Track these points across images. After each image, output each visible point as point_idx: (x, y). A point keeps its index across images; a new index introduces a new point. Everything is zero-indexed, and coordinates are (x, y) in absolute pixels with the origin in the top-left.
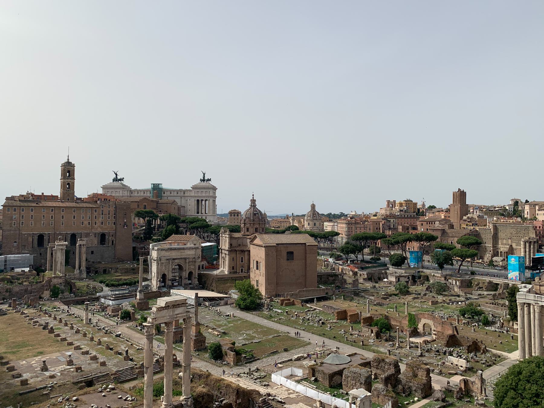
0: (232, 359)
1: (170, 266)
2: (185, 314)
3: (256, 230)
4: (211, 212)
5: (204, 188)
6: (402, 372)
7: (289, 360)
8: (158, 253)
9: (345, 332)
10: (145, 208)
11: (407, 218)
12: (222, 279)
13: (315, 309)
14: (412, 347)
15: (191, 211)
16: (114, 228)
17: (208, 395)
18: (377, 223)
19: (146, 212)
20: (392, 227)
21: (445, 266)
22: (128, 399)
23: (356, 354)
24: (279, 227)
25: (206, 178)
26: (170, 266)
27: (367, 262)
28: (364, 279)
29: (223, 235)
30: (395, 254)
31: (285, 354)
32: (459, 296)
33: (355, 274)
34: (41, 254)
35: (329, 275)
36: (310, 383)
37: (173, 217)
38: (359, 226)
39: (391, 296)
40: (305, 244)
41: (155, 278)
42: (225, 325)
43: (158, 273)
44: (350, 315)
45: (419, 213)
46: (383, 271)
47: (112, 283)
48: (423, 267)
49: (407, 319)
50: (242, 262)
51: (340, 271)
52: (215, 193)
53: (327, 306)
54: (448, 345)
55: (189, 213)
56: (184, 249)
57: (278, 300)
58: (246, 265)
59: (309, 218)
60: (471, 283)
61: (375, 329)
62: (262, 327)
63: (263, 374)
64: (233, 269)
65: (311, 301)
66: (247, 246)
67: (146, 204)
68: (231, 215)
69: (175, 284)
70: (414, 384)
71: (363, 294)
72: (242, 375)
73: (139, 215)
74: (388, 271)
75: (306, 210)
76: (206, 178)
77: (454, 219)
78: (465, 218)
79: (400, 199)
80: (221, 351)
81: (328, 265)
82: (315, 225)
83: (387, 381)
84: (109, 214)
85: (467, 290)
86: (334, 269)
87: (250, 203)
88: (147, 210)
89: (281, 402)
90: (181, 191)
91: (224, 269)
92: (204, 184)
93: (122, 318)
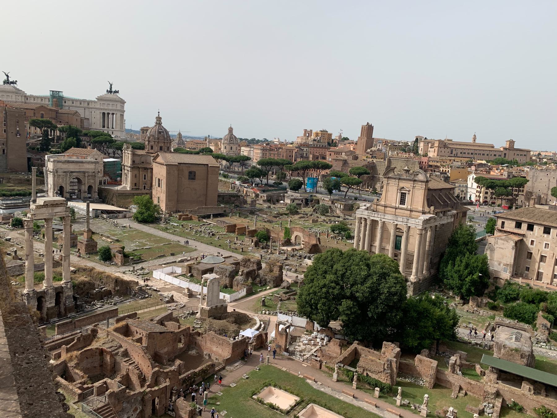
1: (68, 179)
3: (161, 149)
4: (118, 127)
5: (111, 101)
7: (173, 262)
8: (54, 165)
9: (230, 242)
10: (42, 117)
11: (319, 147)
12: (124, 195)
13: (210, 224)
14: (282, 253)
15: (96, 124)
16: (5, 136)
17: (89, 283)
18: (291, 151)
19: (43, 122)
20: (305, 155)
21: (334, 191)
23: (231, 256)
24: (195, 149)
25: (113, 90)
26: (68, 179)
27: (271, 186)
28: (264, 201)
29: (126, 152)
30: (294, 180)
31: (172, 257)
32: (339, 217)
33: (257, 196)
35: (232, 196)
36: (187, 278)
37: (73, 129)
38: (272, 152)
39: (282, 215)
41: (52, 190)
42: (120, 234)
43: (54, 185)
45: (332, 143)
46: (282, 195)
47: (4, 192)
48: (317, 192)
49: (284, 232)
50: (145, 179)
51: (245, 193)
52: (123, 107)
53: (221, 221)
54: (310, 252)
55: (94, 127)
56: (82, 162)
57: (177, 215)
58: (149, 183)
59: (226, 142)
60: (353, 207)
61: (255, 239)
62: (155, 236)
63: (146, 271)
65: (208, 217)
66: (150, 164)
67: (43, 112)
68: (143, 133)
69: (73, 197)
70: (269, 277)
71: (258, 213)
72: (127, 272)
73: (34, 123)
74: (286, 194)
75: (223, 133)
76: (113, 90)
77: (359, 152)
78: (369, 150)
79: (316, 129)
80: (110, 254)
81: (234, 187)
83: (249, 274)
85: (348, 213)
86: (239, 191)
88: (44, 119)
89: (156, 290)
90: (84, 101)
91: (126, 185)
92: (111, 96)
93: (13, 225)
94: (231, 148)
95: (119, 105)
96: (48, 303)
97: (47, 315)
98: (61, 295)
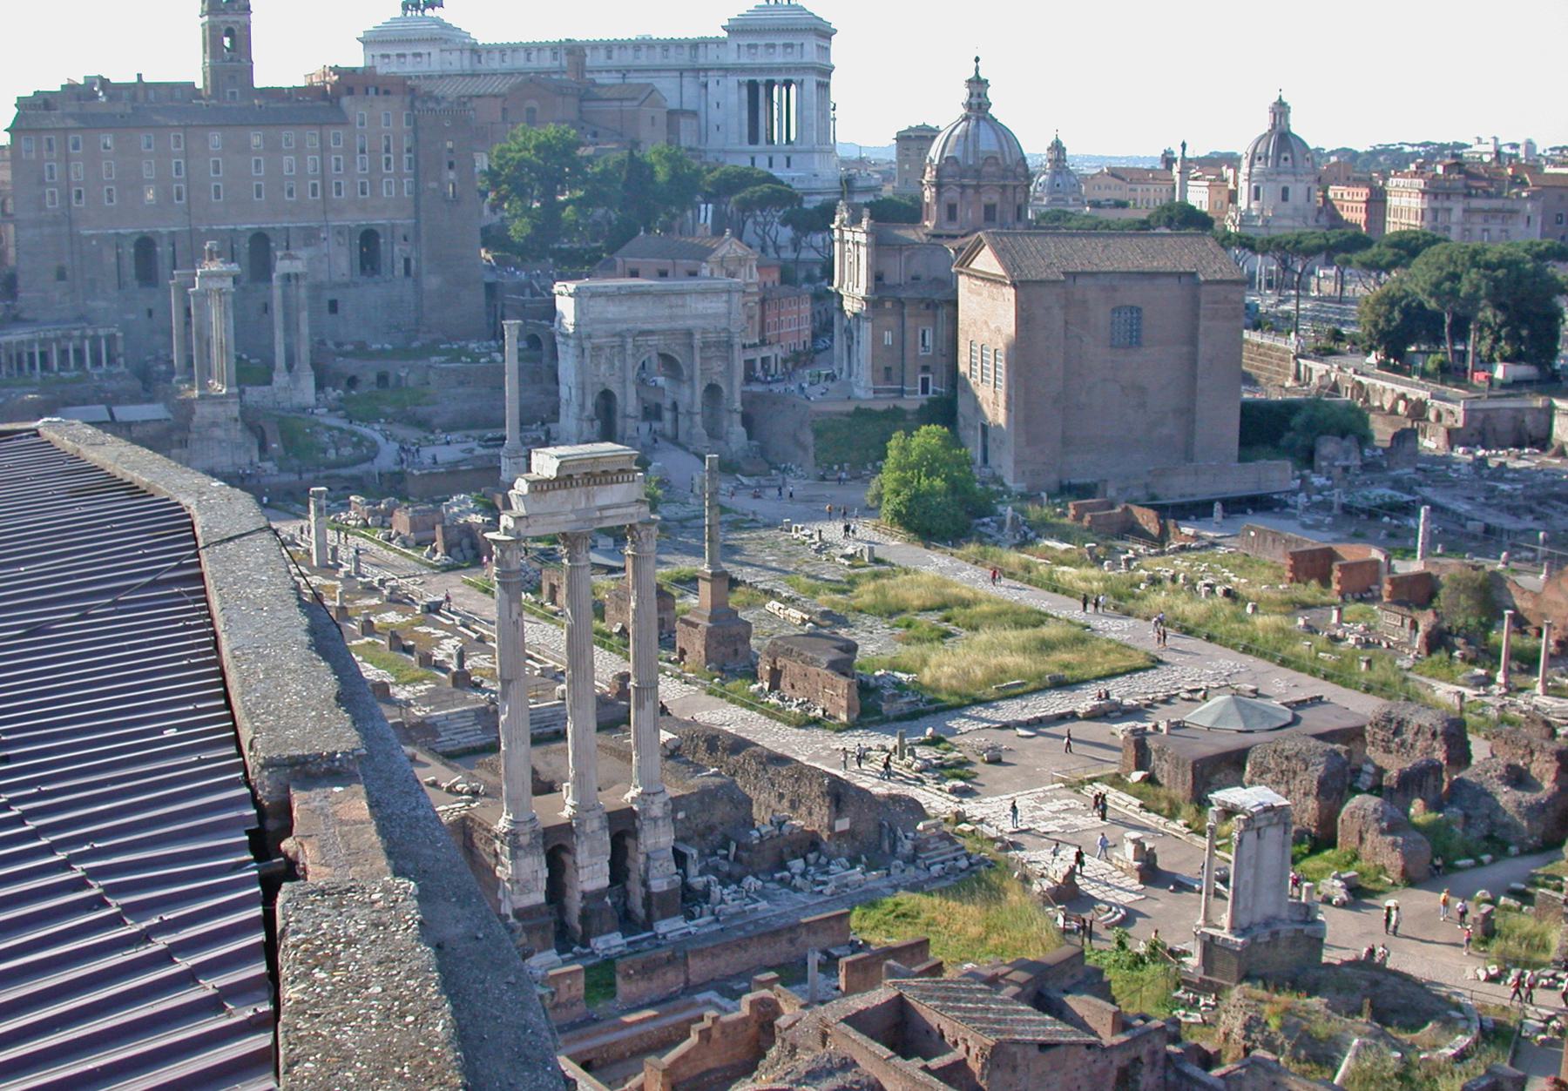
0: (844, 703)
1: (630, 361)
2: (631, 510)
3: (990, 213)
6: (1473, 762)
8: (580, 310)
22: (459, 787)
24: (1121, 205)
34: (150, 313)
40: (1194, 274)
41: (574, 409)
43: (582, 388)
44: (1346, 568)
61: (1426, 620)
64: (888, 378)
67: (534, 104)
75: (1242, 132)
82: (1285, 198)
84: (388, 150)
87: (964, 94)
94: (1285, 191)
95: (811, 43)
96: (583, 875)
97: (585, 916)
98: (629, 842)
